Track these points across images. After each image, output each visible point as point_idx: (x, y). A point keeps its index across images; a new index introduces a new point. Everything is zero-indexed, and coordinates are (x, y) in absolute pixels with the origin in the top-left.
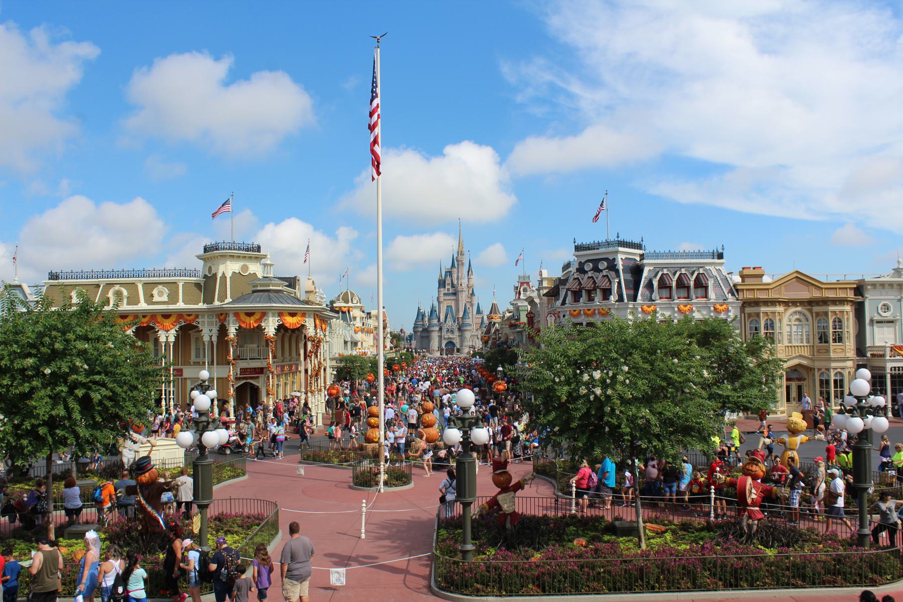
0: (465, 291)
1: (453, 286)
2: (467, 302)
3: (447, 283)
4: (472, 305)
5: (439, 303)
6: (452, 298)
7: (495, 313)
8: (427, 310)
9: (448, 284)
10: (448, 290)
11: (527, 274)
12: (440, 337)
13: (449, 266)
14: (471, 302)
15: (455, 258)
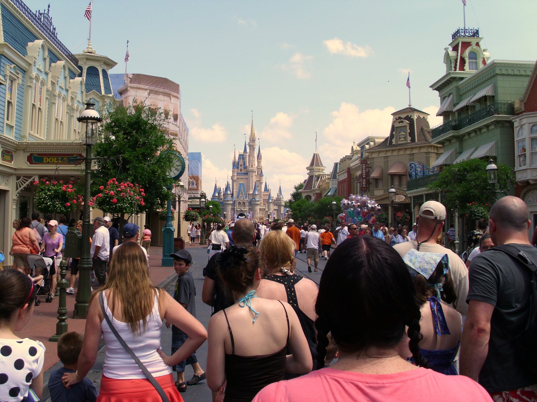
0: (255, 171)
1: (245, 168)
2: (257, 181)
3: (240, 164)
4: (261, 183)
5: (233, 181)
6: (244, 177)
7: (318, 165)
8: (223, 187)
9: (241, 165)
10: (241, 170)
11: (471, 26)
12: (233, 209)
13: (242, 152)
14: (259, 181)
15: (247, 143)
